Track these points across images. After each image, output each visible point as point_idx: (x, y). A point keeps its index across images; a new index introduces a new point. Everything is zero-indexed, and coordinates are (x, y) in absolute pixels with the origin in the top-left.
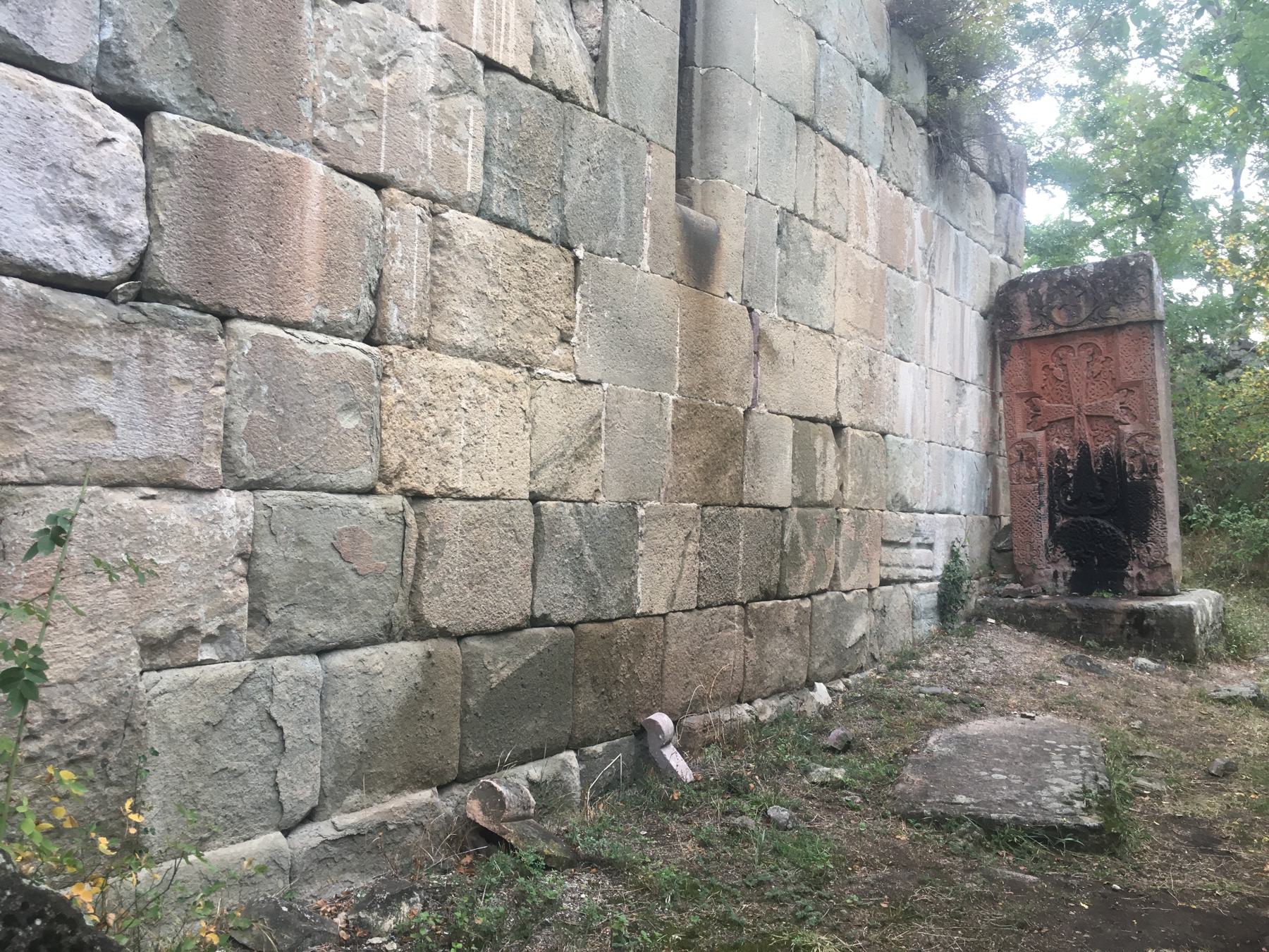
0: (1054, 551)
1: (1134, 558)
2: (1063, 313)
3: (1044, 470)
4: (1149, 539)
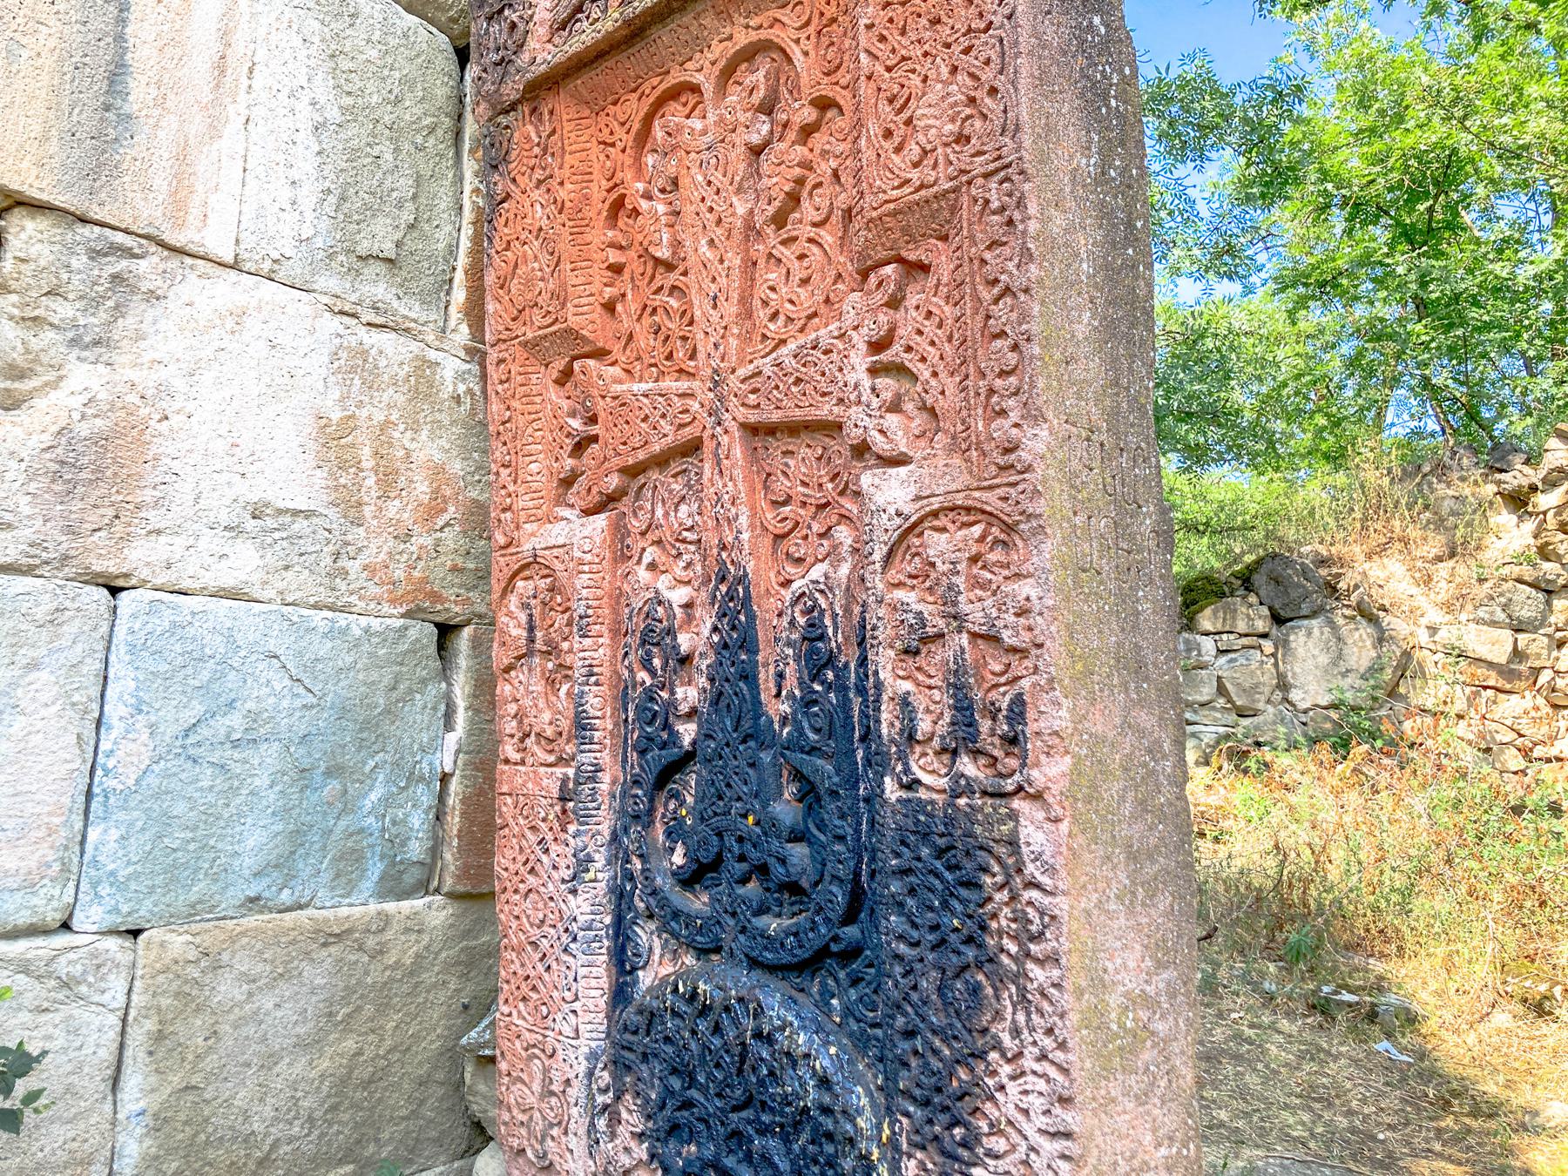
3: (596, 702)
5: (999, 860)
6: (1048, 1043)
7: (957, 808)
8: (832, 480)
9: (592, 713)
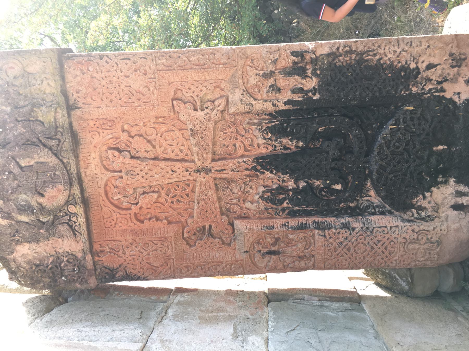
0: (421, 208)
1: (443, 90)
2: (50, 192)
4: (413, 66)
5: (333, 60)
6: (376, 45)
7: (320, 74)
8: (230, 128)
9: (297, 224)
